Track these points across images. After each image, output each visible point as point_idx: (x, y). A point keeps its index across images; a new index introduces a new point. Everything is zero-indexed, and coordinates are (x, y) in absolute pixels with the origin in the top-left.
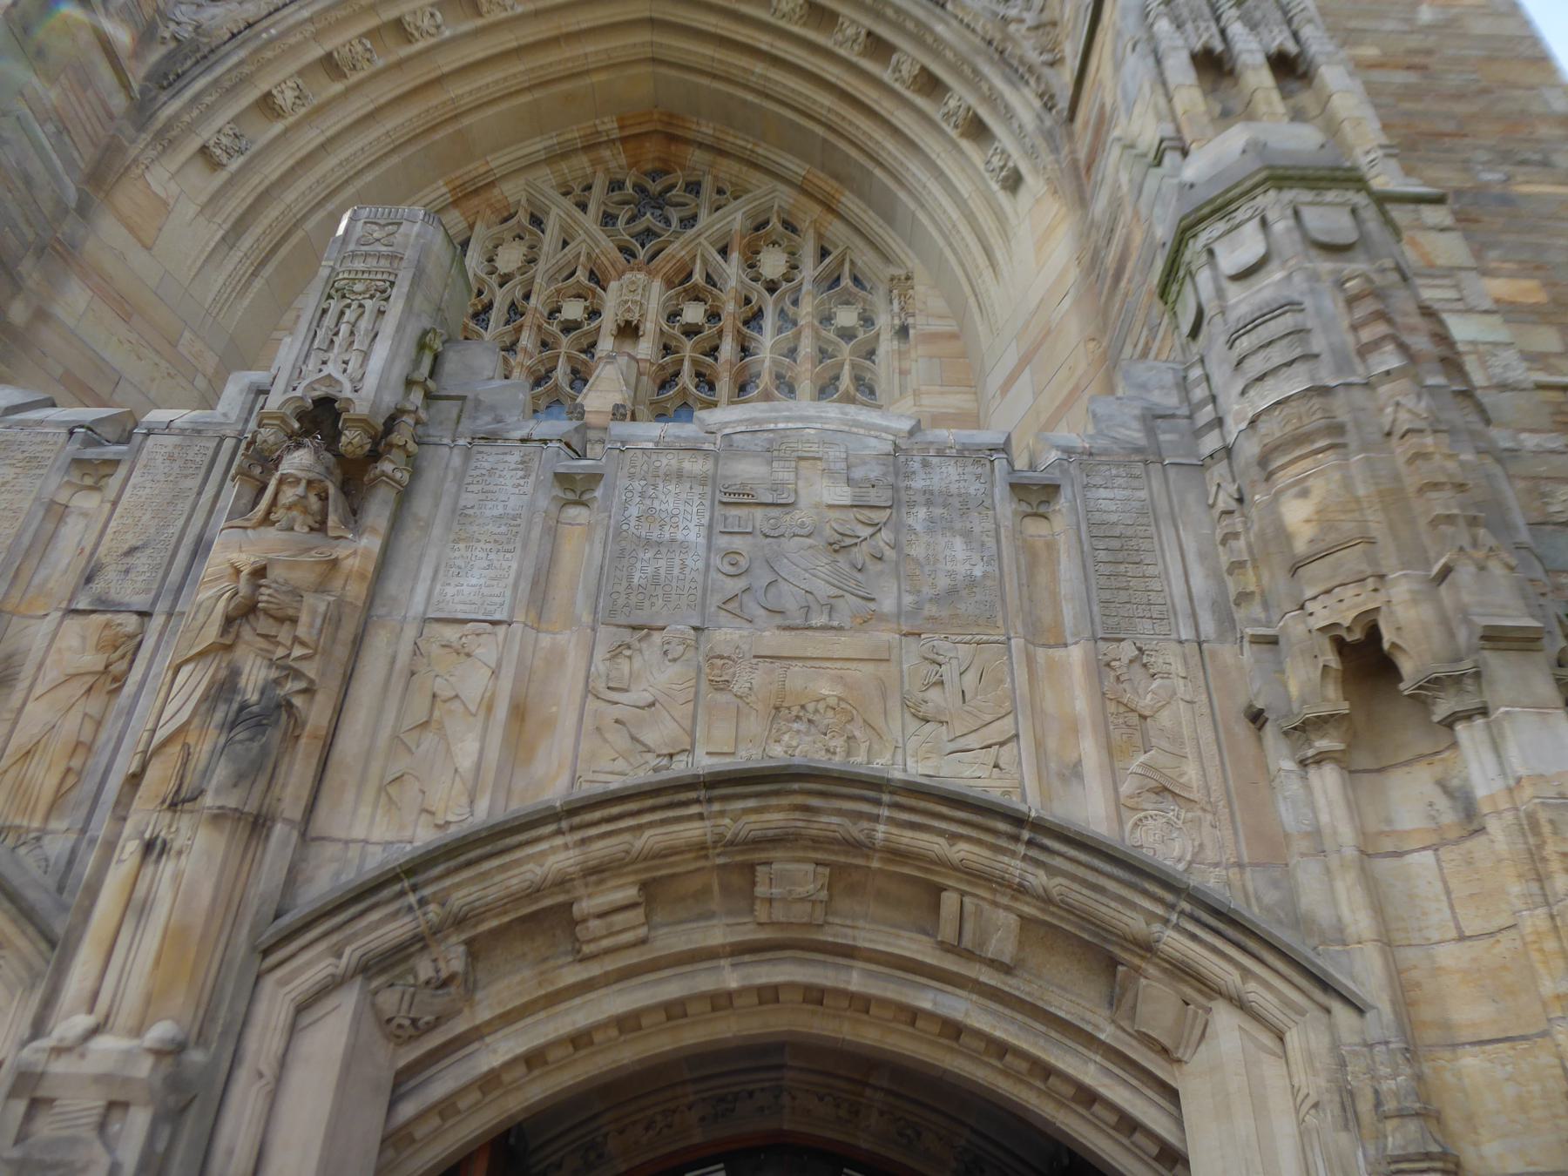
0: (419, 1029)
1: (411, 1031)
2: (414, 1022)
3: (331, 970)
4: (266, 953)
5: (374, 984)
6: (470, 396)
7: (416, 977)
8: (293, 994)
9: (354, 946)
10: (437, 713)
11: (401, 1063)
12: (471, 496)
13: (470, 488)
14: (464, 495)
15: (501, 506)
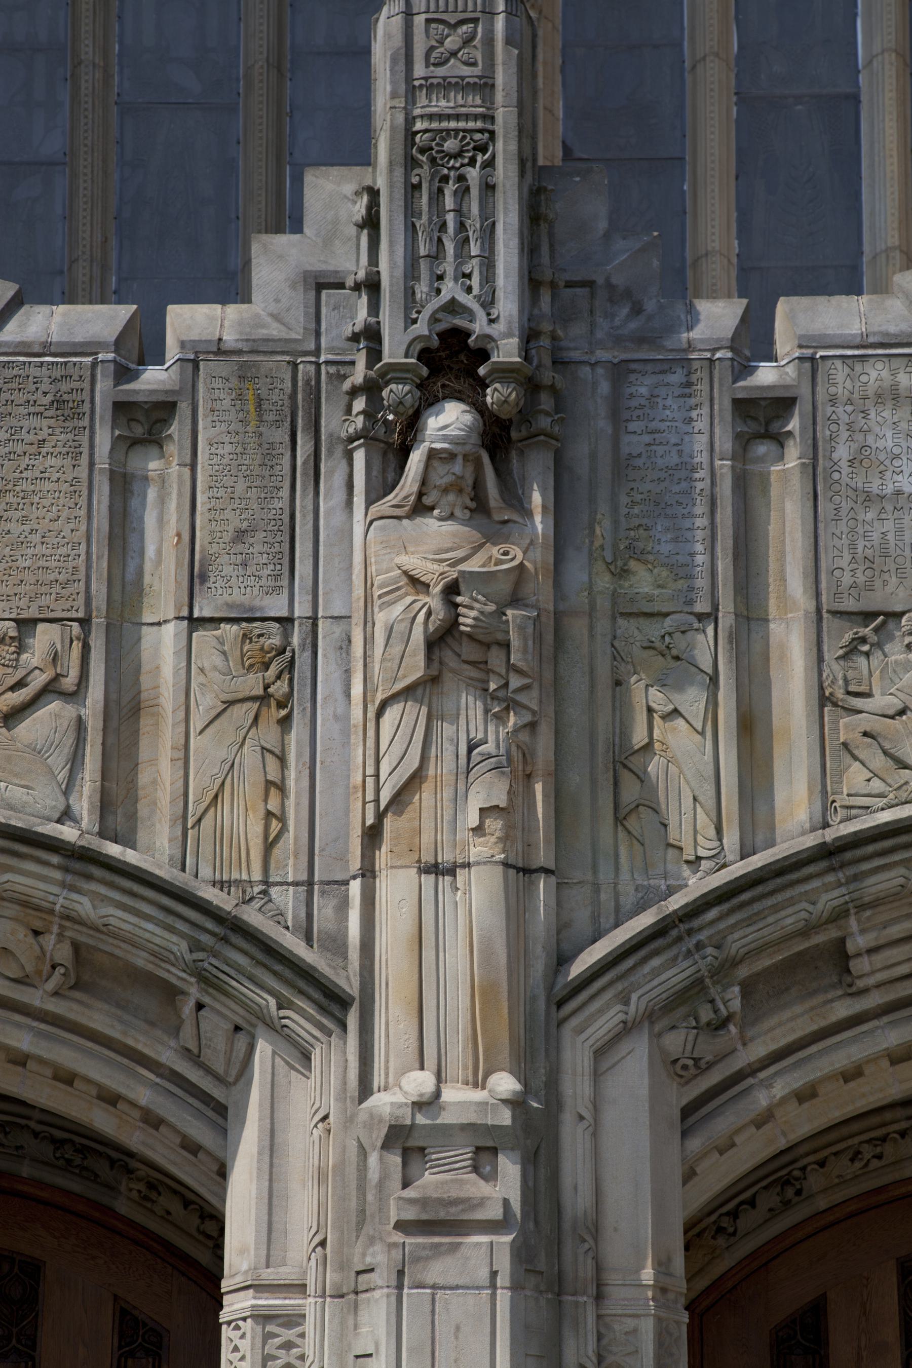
0: (701, 1067)
1: (693, 1071)
2: (696, 1060)
3: (621, 1017)
4: (560, 1004)
5: (657, 1028)
6: (600, 281)
7: (696, 1019)
8: (591, 1041)
9: (640, 992)
10: (656, 733)
11: (684, 1101)
12: (634, 438)
13: (632, 426)
14: (626, 439)
15: (674, 454)
